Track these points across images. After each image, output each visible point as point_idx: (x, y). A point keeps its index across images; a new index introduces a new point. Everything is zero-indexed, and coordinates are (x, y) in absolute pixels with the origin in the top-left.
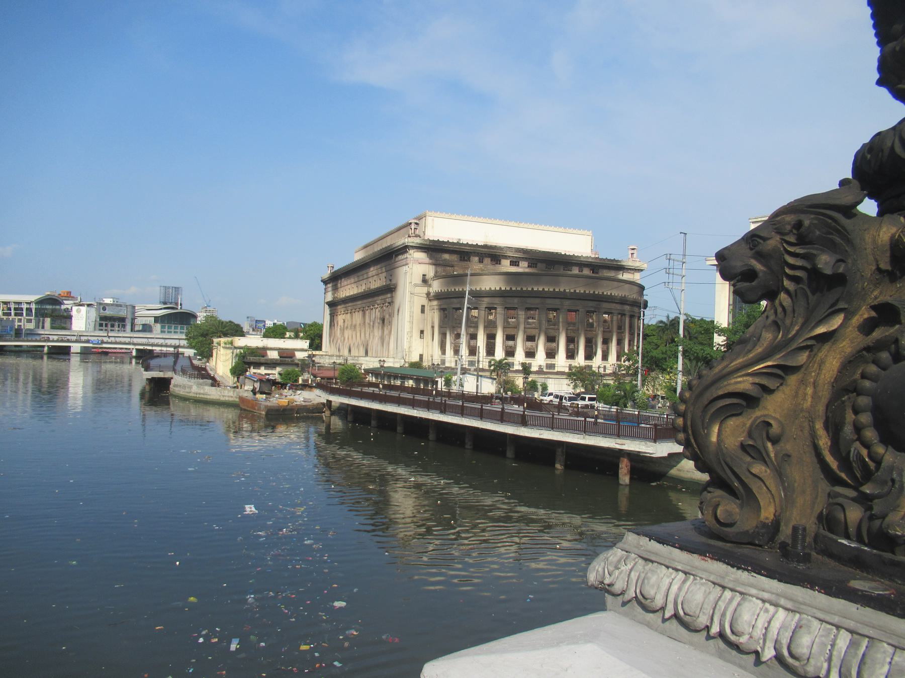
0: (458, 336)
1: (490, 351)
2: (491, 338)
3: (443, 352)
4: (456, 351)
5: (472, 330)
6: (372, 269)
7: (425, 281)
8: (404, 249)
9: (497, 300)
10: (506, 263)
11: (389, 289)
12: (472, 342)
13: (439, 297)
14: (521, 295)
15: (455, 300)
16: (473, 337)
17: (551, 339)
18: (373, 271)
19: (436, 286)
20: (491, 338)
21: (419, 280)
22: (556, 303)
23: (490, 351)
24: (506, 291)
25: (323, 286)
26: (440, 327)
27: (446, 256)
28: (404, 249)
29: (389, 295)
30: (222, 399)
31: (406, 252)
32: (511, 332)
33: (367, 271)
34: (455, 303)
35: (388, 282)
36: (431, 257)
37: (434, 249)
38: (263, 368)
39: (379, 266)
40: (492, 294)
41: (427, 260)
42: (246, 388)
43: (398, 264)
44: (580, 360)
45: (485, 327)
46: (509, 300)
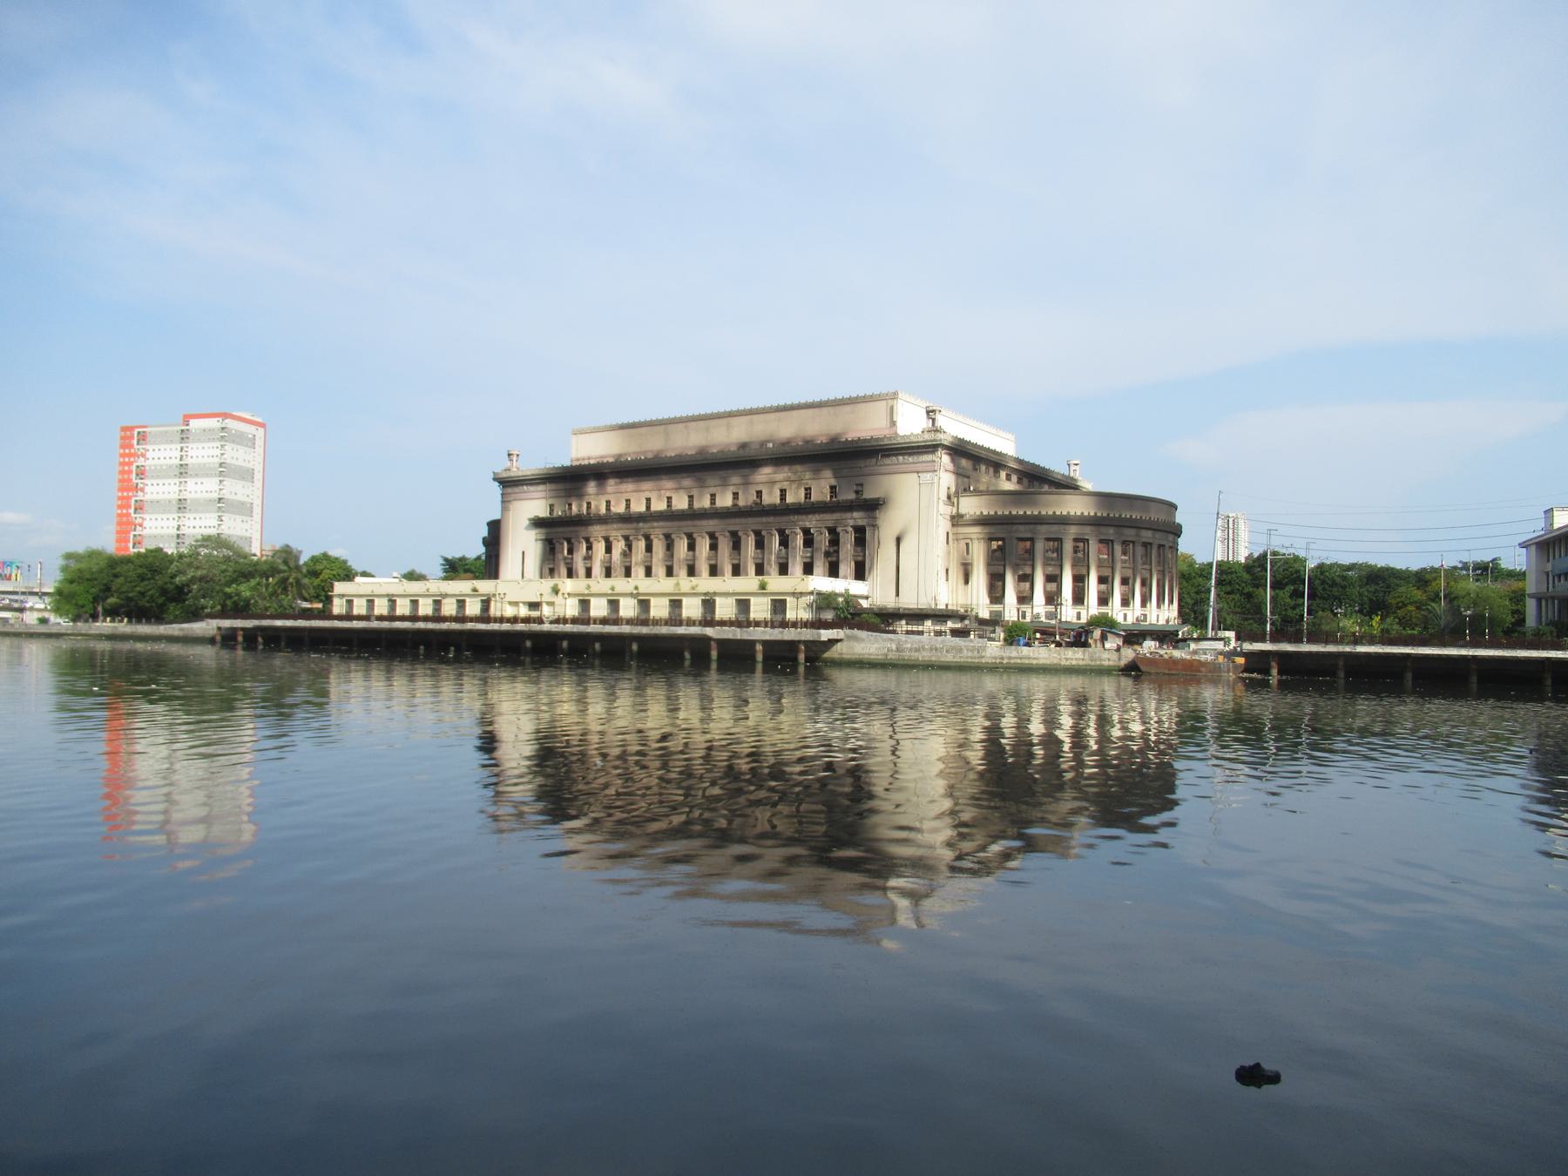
0: (1027, 578)
1: (1079, 598)
2: (1079, 580)
3: (996, 595)
4: (1025, 599)
5: (1050, 570)
6: (767, 470)
7: (949, 497)
8: (932, 448)
9: (1088, 529)
10: (1003, 474)
11: (873, 506)
12: (1052, 587)
13: (982, 521)
14: (1120, 524)
15: (1021, 528)
16: (1053, 578)
17: (1145, 583)
18: (765, 473)
19: (971, 506)
20: (1079, 580)
21: (944, 497)
22: (1147, 535)
23: (1079, 598)
24: (1102, 518)
25: (496, 489)
26: (989, 564)
27: (964, 462)
28: (932, 448)
29: (855, 514)
30: (1063, 663)
31: (933, 452)
32: (1107, 572)
33: (746, 471)
34: (1023, 531)
35: (852, 496)
36: (953, 461)
37: (960, 450)
38: (928, 623)
39: (798, 468)
40: (1083, 521)
41: (950, 466)
42: (1107, 645)
43: (883, 469)
44: (1092, 608)
45: (1073, 566)
46: (1103, 529)
